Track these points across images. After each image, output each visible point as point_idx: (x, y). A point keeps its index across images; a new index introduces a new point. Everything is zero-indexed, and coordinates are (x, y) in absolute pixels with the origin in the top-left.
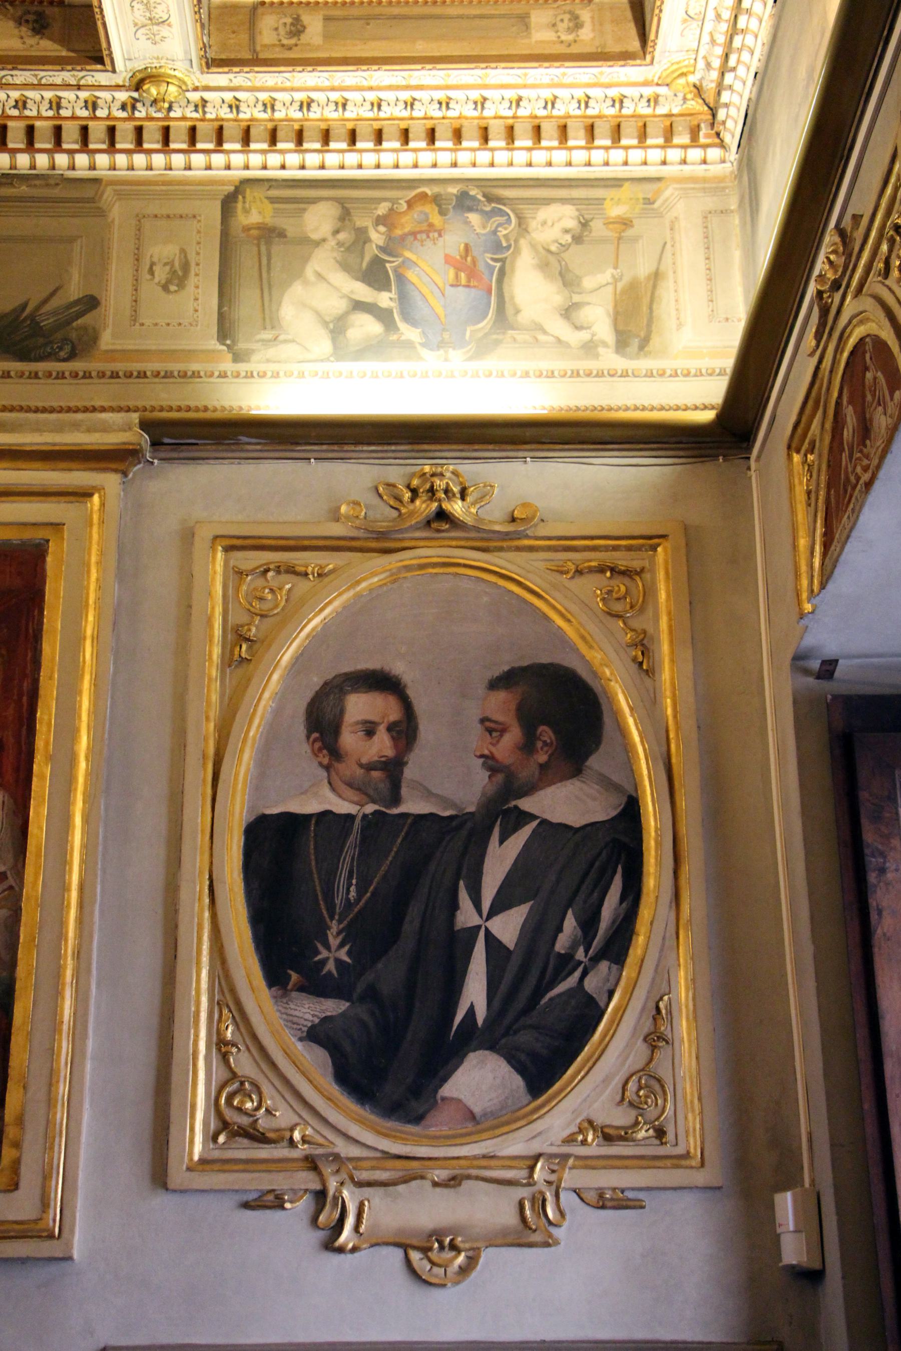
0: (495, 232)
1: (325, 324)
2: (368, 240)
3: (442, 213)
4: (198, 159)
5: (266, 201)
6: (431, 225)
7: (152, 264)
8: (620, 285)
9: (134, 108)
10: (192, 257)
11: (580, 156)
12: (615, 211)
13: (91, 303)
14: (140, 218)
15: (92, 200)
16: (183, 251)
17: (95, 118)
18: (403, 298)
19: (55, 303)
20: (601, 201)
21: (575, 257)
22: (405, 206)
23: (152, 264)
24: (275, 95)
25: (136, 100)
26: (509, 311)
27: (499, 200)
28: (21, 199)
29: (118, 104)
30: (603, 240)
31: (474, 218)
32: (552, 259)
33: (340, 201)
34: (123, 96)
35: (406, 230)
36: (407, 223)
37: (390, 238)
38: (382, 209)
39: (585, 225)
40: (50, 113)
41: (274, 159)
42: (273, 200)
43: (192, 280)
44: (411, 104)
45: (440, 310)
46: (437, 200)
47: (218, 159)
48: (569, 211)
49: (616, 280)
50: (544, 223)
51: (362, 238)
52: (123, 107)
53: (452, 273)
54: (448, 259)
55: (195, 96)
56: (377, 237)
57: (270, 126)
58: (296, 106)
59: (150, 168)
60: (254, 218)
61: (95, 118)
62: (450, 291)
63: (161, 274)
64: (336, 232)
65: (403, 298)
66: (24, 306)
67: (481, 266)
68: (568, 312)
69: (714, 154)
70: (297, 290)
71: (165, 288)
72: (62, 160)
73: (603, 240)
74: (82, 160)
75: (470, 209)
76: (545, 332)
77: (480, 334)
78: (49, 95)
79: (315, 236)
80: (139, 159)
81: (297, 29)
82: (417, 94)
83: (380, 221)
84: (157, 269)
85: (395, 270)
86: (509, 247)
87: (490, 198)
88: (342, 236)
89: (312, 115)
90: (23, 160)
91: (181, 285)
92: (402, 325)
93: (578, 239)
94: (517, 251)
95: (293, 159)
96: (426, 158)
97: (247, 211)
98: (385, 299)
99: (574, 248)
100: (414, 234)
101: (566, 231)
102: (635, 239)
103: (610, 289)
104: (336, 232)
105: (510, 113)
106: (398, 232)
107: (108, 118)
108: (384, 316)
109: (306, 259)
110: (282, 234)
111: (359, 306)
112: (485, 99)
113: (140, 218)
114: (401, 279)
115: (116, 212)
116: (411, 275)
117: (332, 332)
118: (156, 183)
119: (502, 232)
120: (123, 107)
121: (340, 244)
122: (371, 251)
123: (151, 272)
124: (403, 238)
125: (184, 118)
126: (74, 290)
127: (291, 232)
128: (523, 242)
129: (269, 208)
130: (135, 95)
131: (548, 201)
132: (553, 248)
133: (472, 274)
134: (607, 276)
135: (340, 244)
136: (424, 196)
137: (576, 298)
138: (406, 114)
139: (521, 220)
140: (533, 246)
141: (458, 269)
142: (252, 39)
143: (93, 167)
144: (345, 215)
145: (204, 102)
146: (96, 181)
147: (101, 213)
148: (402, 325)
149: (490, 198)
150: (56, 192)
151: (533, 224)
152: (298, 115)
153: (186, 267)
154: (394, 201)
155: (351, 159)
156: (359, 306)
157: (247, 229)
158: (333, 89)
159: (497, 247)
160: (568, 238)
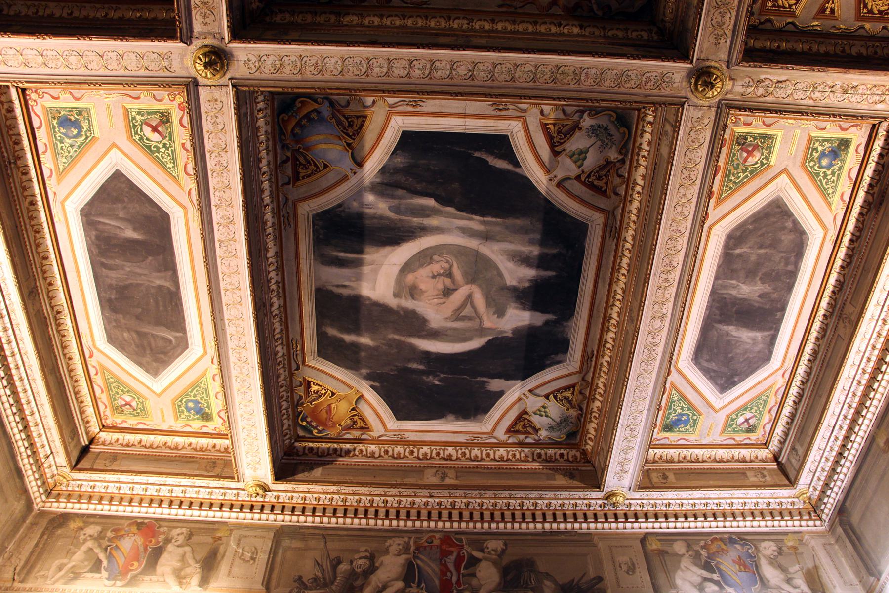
0: (748, 551)
1: (695, 587)
2: (701, 555)
3: (725, 544)
4: (628, 525)
5: (657, 541)
6: (723, 549)
7: (620, 564)
8: (804, 571)
9: (604, 506)
10: (634, 561)
11: (769, 523)
12: (790, 544)
13: (600, 579)
14: (610, 547)
15: (590, 541)
16: (630, 559)
17: (589, 510)
18: (722, 575)
19: (584, 580)
20: (782, 540)
21: (782, 560)
22: (710, 542)
23: (620, 564)
24: (657, 501)
25: (605, 503)
26: (766, 582)
27: (745, 540)
28: (562, 540)
29: (598, 505)
30: (790, 554)
31: (737, 546)
32: (774, 562)
33: (685, 540)
34: (600, 502)
35: (714, 550)
36: (714, 548)
37: (709, 554)
38: (702, 543)
39: (780, 548)
40: (573, 509)
41: (657, 525)
42: (660, 540)
43: (637, 570)
44: (706, 504)
45: (738, 581)
46: (721, 539)
47: (636, 525)
48: (772, 543)
49: (802, 569)
50: (765, 548)
51: (697, 555)
52: (600, 506)
53: (737, 567)
54: (734, 561)
55: (627, 502)
56: (704, 553)
57: (654, 512)
58: (664, 505)
59: (610, 529)
60: (654, 547)
61: (589, 510)
62: (739, 573)
63: (624, 568)
64: (688, 552)
65: (722, 575)
66: (573, 580)
67: (747, 563)
68: (789, 581)
69: (818, 523)
70: (679, 573)
71: (628, 573)
72: (577, 526)
73: (790, 554)
74: (584, 526)
75: (736, 543)
76: (783, 589)
77: (758, 590)
78: (572, 502)
79: (680, 553)
80: (606, 525)
81: (665, 477)
82: (708, 501)
83: (703, 547)
84: (623, 566)
85: (715, 566)
86: (755, 557)
87: (742, 539)
88: (690, 553)
89: (670, 509)
90: (562, 526)
91: (634, 572)
92: (726, 587)
93: (780, 554)
94: (759, 558)
95: (664, 525)
96: (714, 524)
97: (651, 545)
98: (715, 576)
99: (780, 557)
100: (718, 552)
101: (774, 551)
102: (802, 554)
103: (800, 572)
104: (688, 552)
105: (742, 508)
106: (711, 551)
107: (594, 510)
108: (717, 583)
109: (679, 562)
110: (667, 553)
111: (706, 579)
112: (733, 503)
113: (610, 547)
114: (718, 569)
115: (600, 545)
116: (722, 567)
117: (699, 589)
118: (613, 534)
119: (751, 552)
120: (600, 506)
121: (691, 556)
122: (704, 559)
123: (620, 567)
124: (714, 553)
125: (622, 510)
126: (592, 574)
127: (670, 551)
128: (759, 555)
129: (659, 543)
130: (606, 502)
131: (763, 540)
132: (772, 557)
133: (745, 567)
134: (797, 567)
135: (691, 556)
136: (716, 538)
137: (789, 576)
138: (704, 508)
139: (756, 547)
140: (764, 556)
141: (740, 565)
142: (650, 480)
143: (588, 528)
144: (689, 546)
145: (630, 504)
146: (590, 534)
147: (595, 545)
148: (726, 587)
149: (742, 539)
150: (576, 538)
151: (761, 549)
152: (665, 509)
153: (633, 565)
154: (706, 540)
155: (686, 525)
156: (706, 579)
157: (653, 551)
158: (678, 499)
159: (751, 557)
160: (776, 553)
